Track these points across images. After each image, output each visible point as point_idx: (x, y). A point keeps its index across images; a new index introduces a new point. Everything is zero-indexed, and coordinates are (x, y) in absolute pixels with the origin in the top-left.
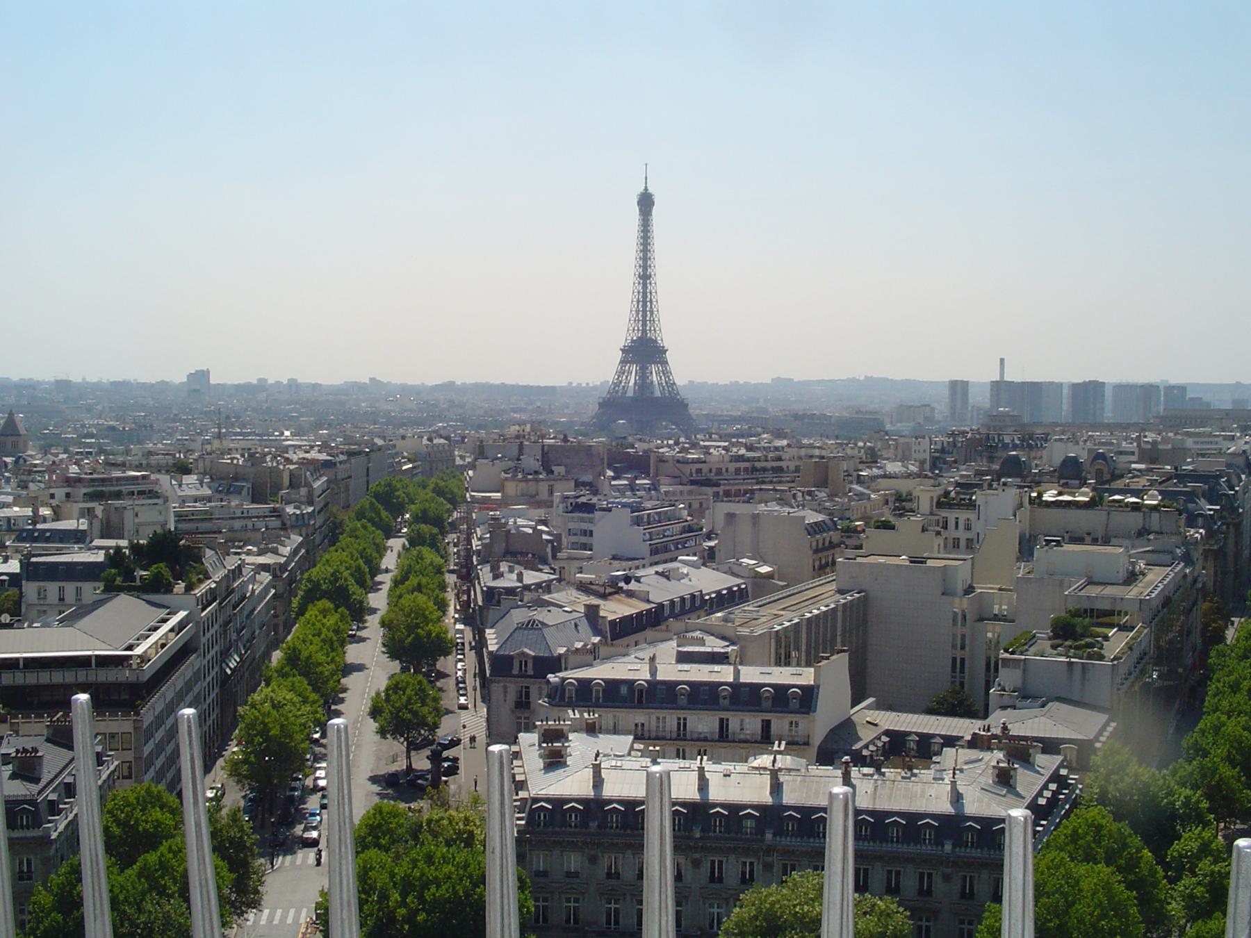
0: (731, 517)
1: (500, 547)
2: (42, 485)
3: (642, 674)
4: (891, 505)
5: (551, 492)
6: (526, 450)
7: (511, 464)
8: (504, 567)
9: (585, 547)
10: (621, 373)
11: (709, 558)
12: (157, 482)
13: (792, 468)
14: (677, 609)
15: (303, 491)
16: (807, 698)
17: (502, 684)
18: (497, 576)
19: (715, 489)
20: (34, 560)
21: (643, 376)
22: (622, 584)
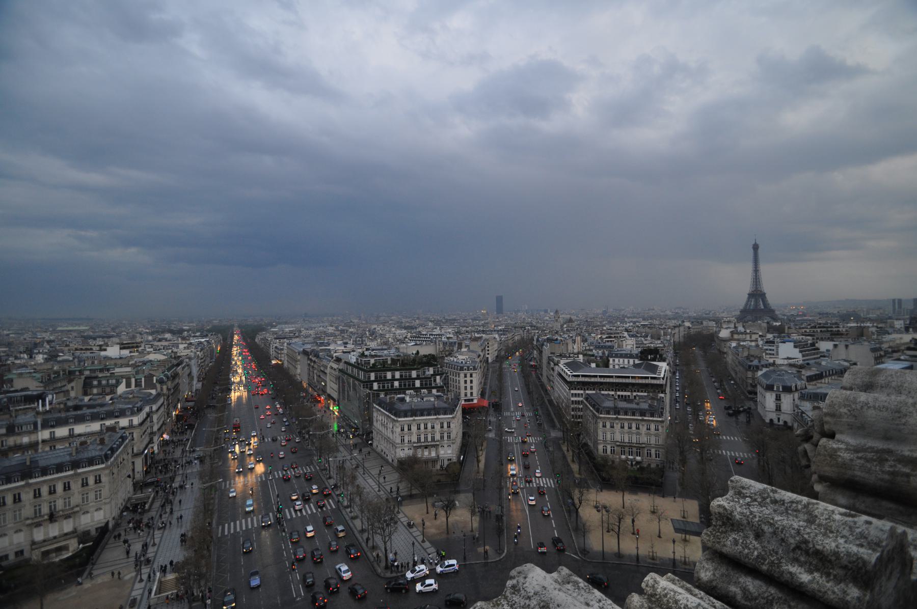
0: (835, 346)
5: (751, 337)
18: (752, 361)
21: (756, 301)
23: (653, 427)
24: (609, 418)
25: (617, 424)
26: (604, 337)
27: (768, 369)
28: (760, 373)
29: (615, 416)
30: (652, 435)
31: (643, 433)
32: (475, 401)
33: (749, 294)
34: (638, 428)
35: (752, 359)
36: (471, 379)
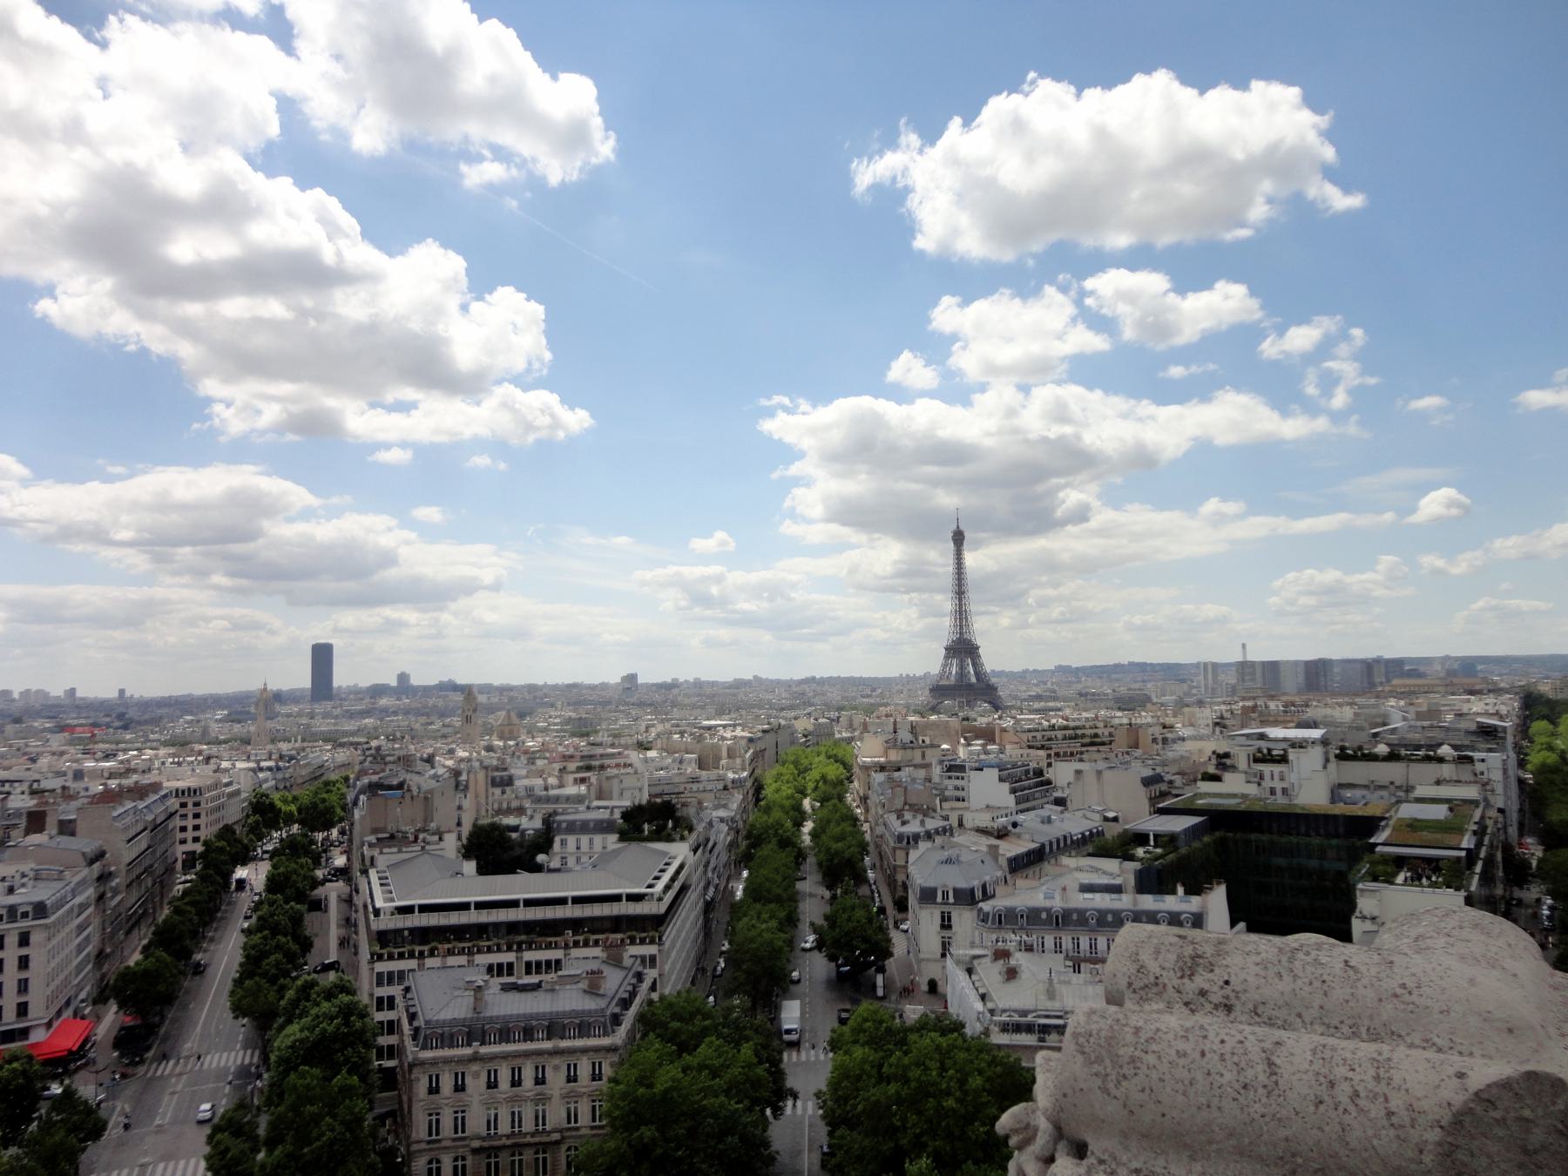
0: (1078, 772)
1: (899, 803)
2: (546, 761)
3: (1057, 904)
4: (1214, 761)
5: (923, 756)
6: (898, 726)
7: (891, 737)
8: (908, 816)
9: (958, 799)
10: (944, 666)
11: (1060, 802)
12: (627, 756)
13: (1106, 733)
14: (1055, 847)
15: (738, 761)
16: (1198, 921)
17: (929, 911)
18: (904, 823)
19: (1049, 752)
20: (558, 818)
21: (962, 667)
22: (1010, 828)
23: (584, 1069)
24: (447, 1061)
25: (476, 1075)
26: (572, 766)
27: (929, 844)
28: (914, 855)
29: (468, 1051)
30: (581, 1095)
31: (556, 1093)
32: (38, 1036)
33: (946, 649)
34: (540, 1081)
35: (908, 816)
36: (24, 951)
